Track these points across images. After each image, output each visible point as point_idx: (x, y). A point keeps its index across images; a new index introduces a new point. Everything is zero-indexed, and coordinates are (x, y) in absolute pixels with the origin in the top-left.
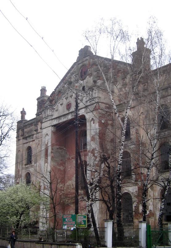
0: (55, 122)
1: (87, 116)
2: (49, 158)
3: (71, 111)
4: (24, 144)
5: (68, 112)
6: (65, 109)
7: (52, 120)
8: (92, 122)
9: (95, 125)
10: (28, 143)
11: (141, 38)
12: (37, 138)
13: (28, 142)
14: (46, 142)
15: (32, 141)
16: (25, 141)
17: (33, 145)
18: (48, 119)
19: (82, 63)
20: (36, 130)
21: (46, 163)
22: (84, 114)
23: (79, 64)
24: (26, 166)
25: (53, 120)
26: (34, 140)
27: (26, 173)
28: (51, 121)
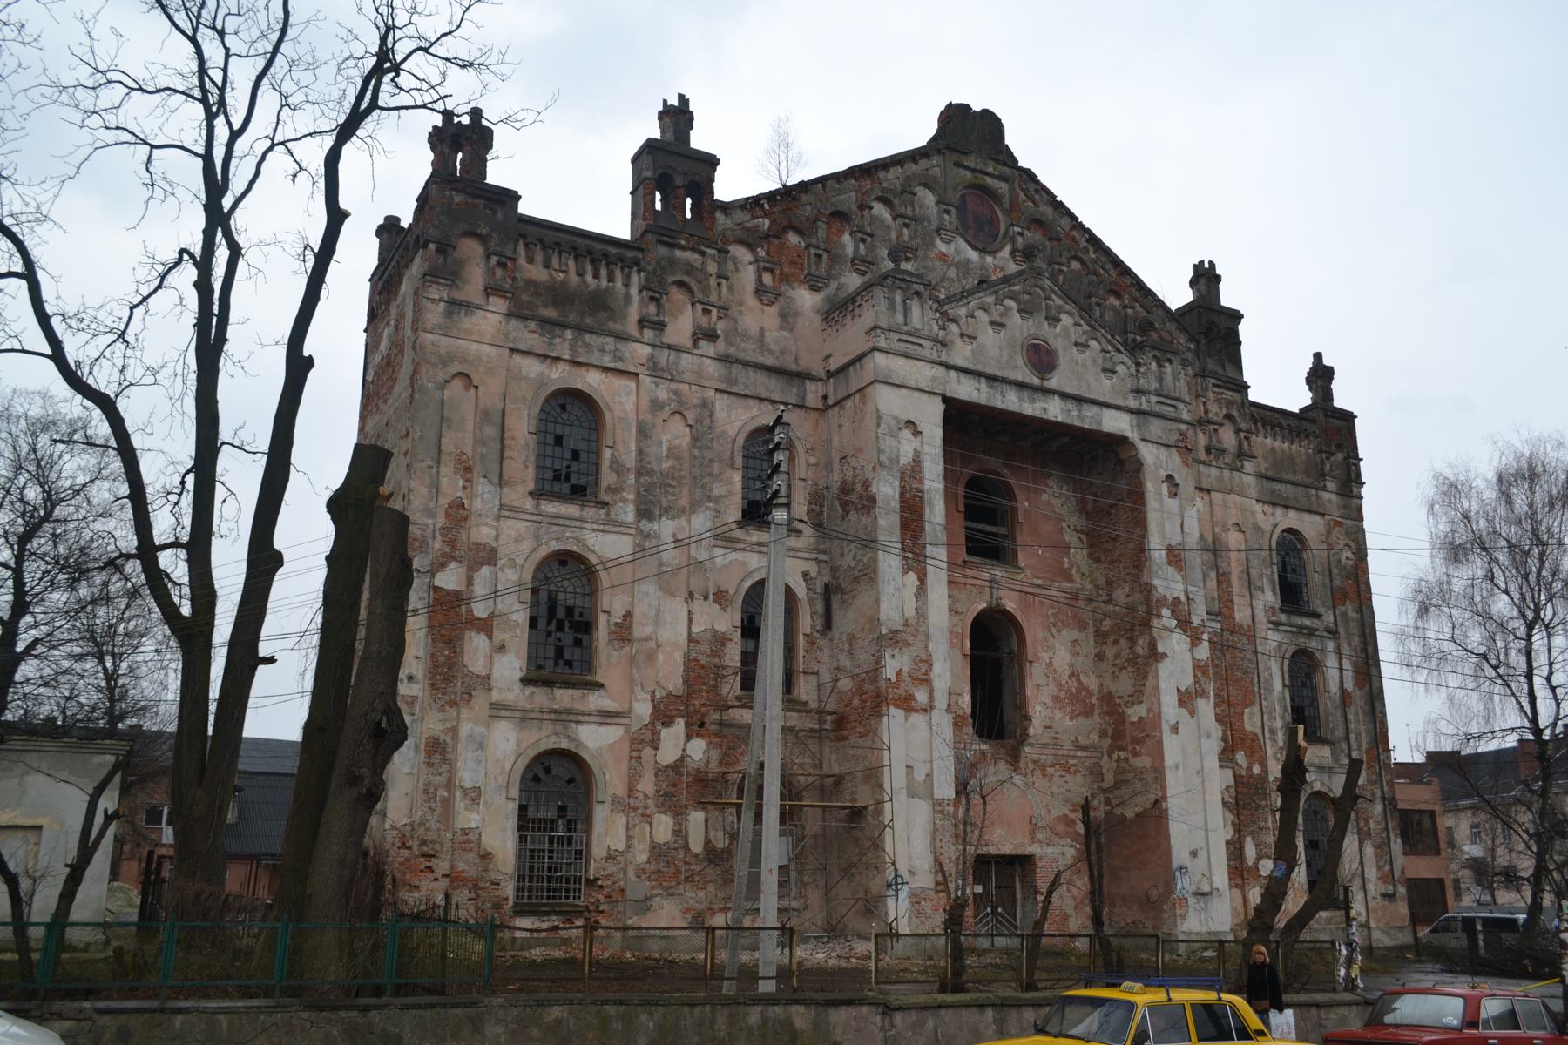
0: (967, 390)
1: (1147, 453)
2: (938, 555)
3: (1053, 383)
4: (517, 358)
5: (1036, 381)
6: (1020, 361)
7: (948, 367)
8: (1165, 486)
9: (1182, 508)
10: (562, 366)
11: (1211, 263)
12: (655, 370)
13: (557, 359)
14: (906, 458)
15: (606, 369)
16: (529, 337)
17: (621, 400)
18: (926, 353)
19: (973, 171)
20: (660, 326)
21: (912, 577)
22: (1129, 434)
23: (958, 165)
24: (550, 507)
25: (953, 373)
26: (637, 375)
27: (543, 552)
28: (942, 370)
